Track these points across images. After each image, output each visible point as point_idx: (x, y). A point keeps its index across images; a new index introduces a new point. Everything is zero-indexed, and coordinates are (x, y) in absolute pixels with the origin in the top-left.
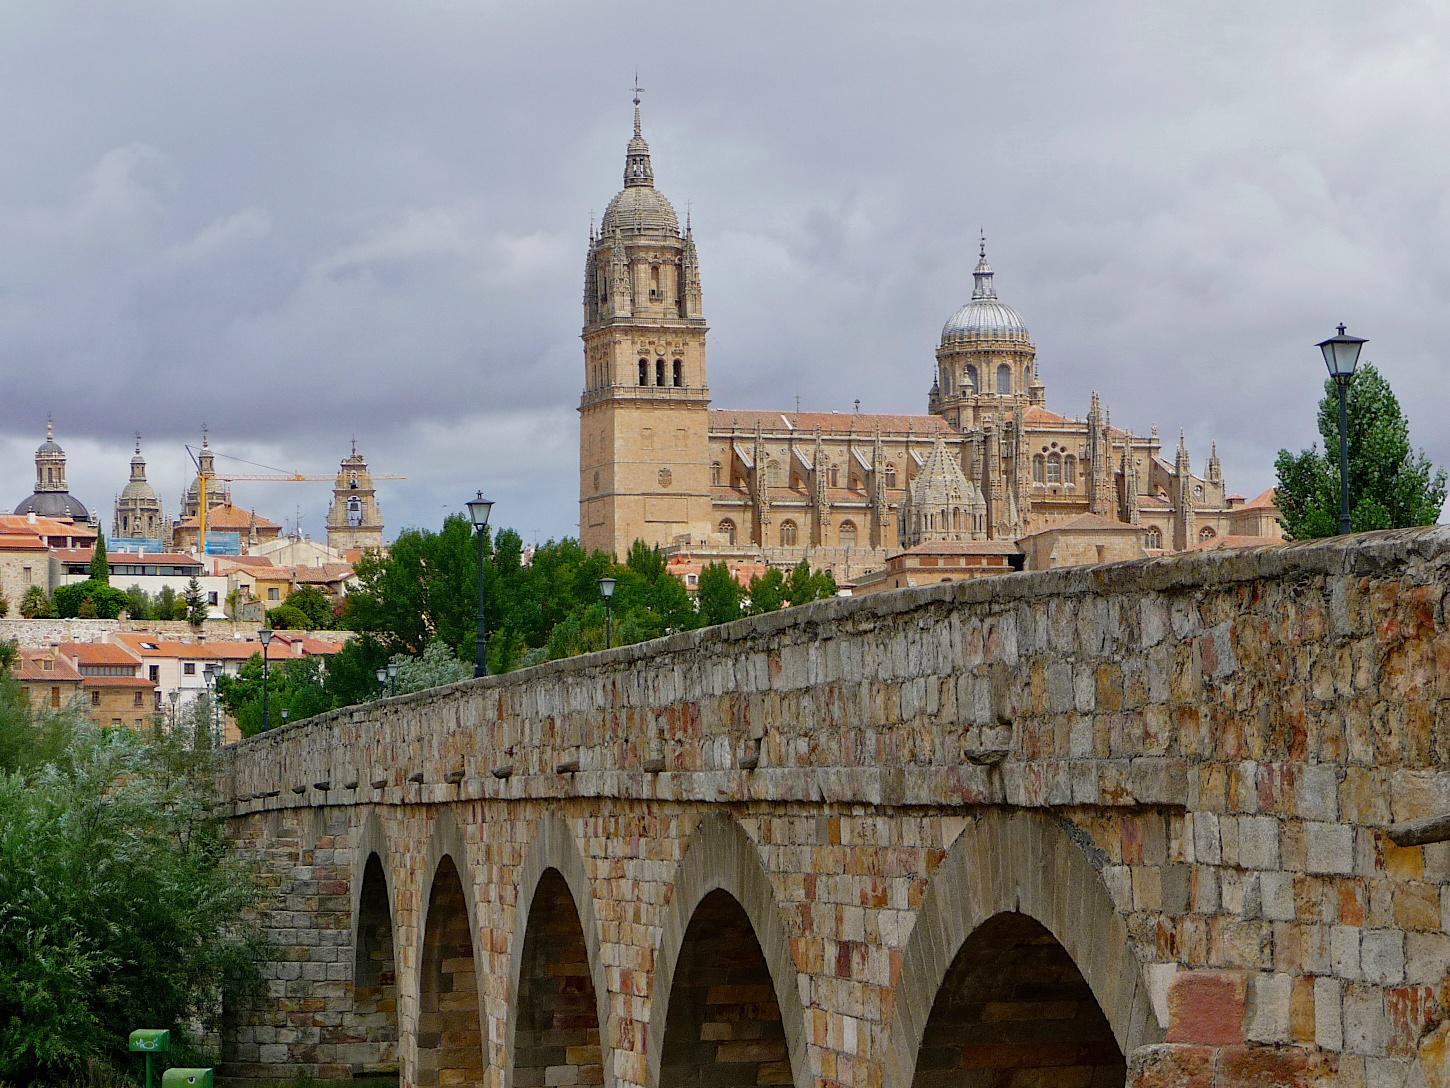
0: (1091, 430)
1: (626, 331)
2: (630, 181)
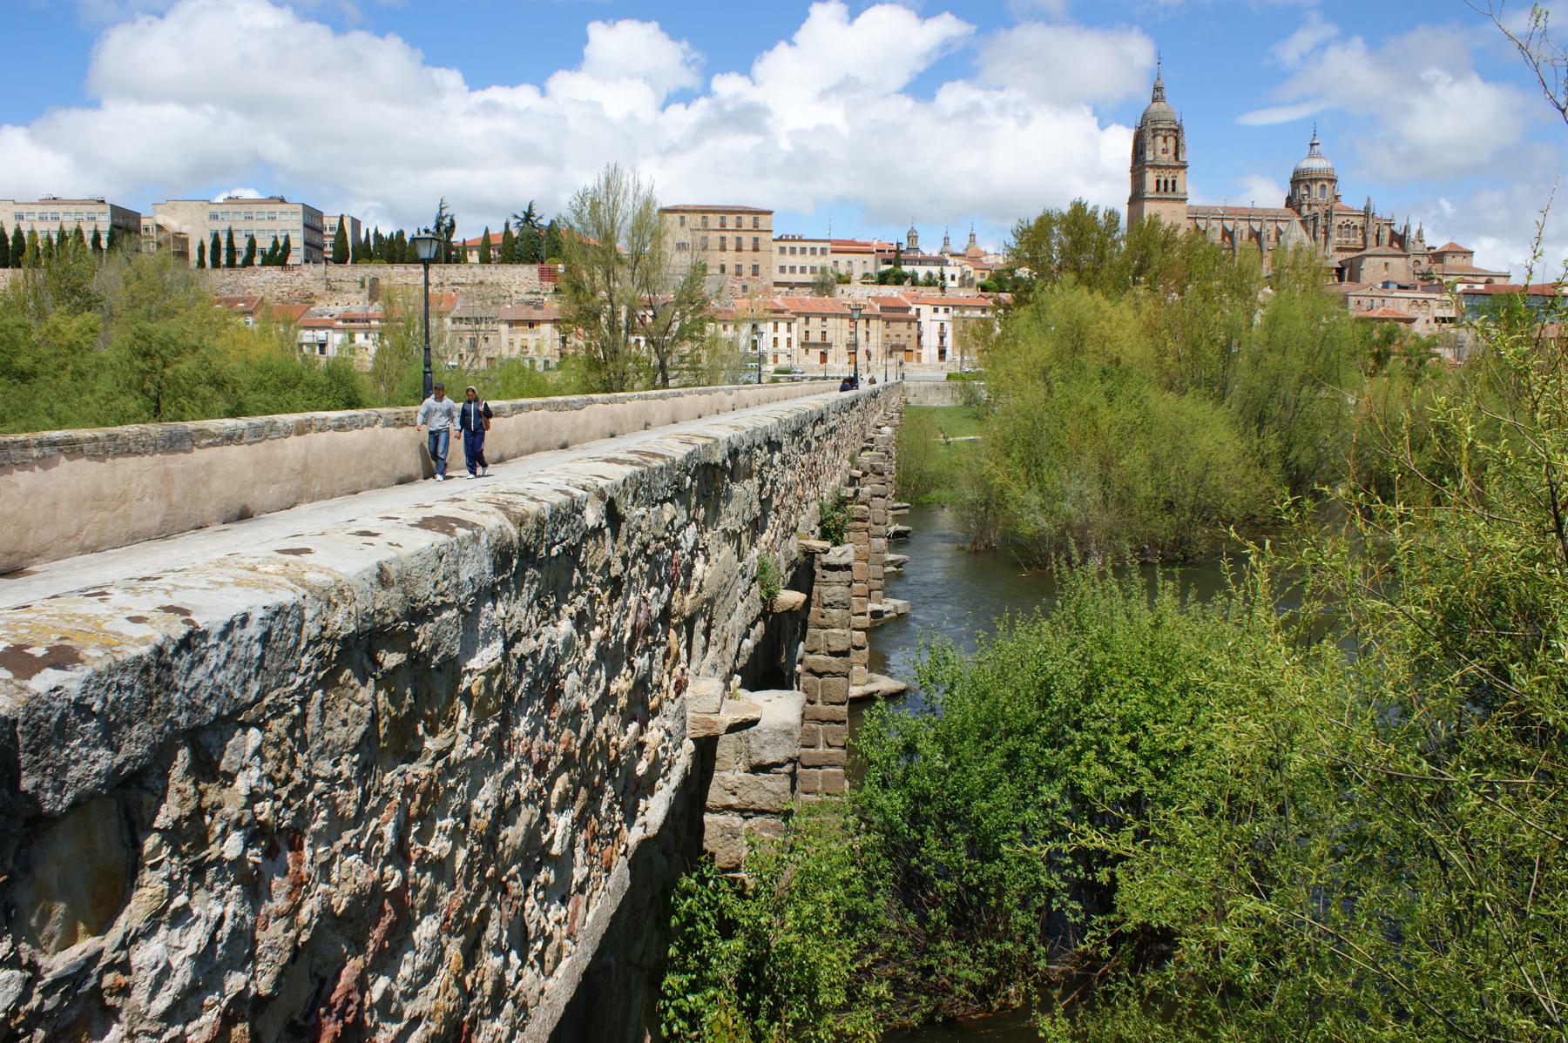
0: (1367, 214)
1: (1151, 167)
2: (1154, 100)
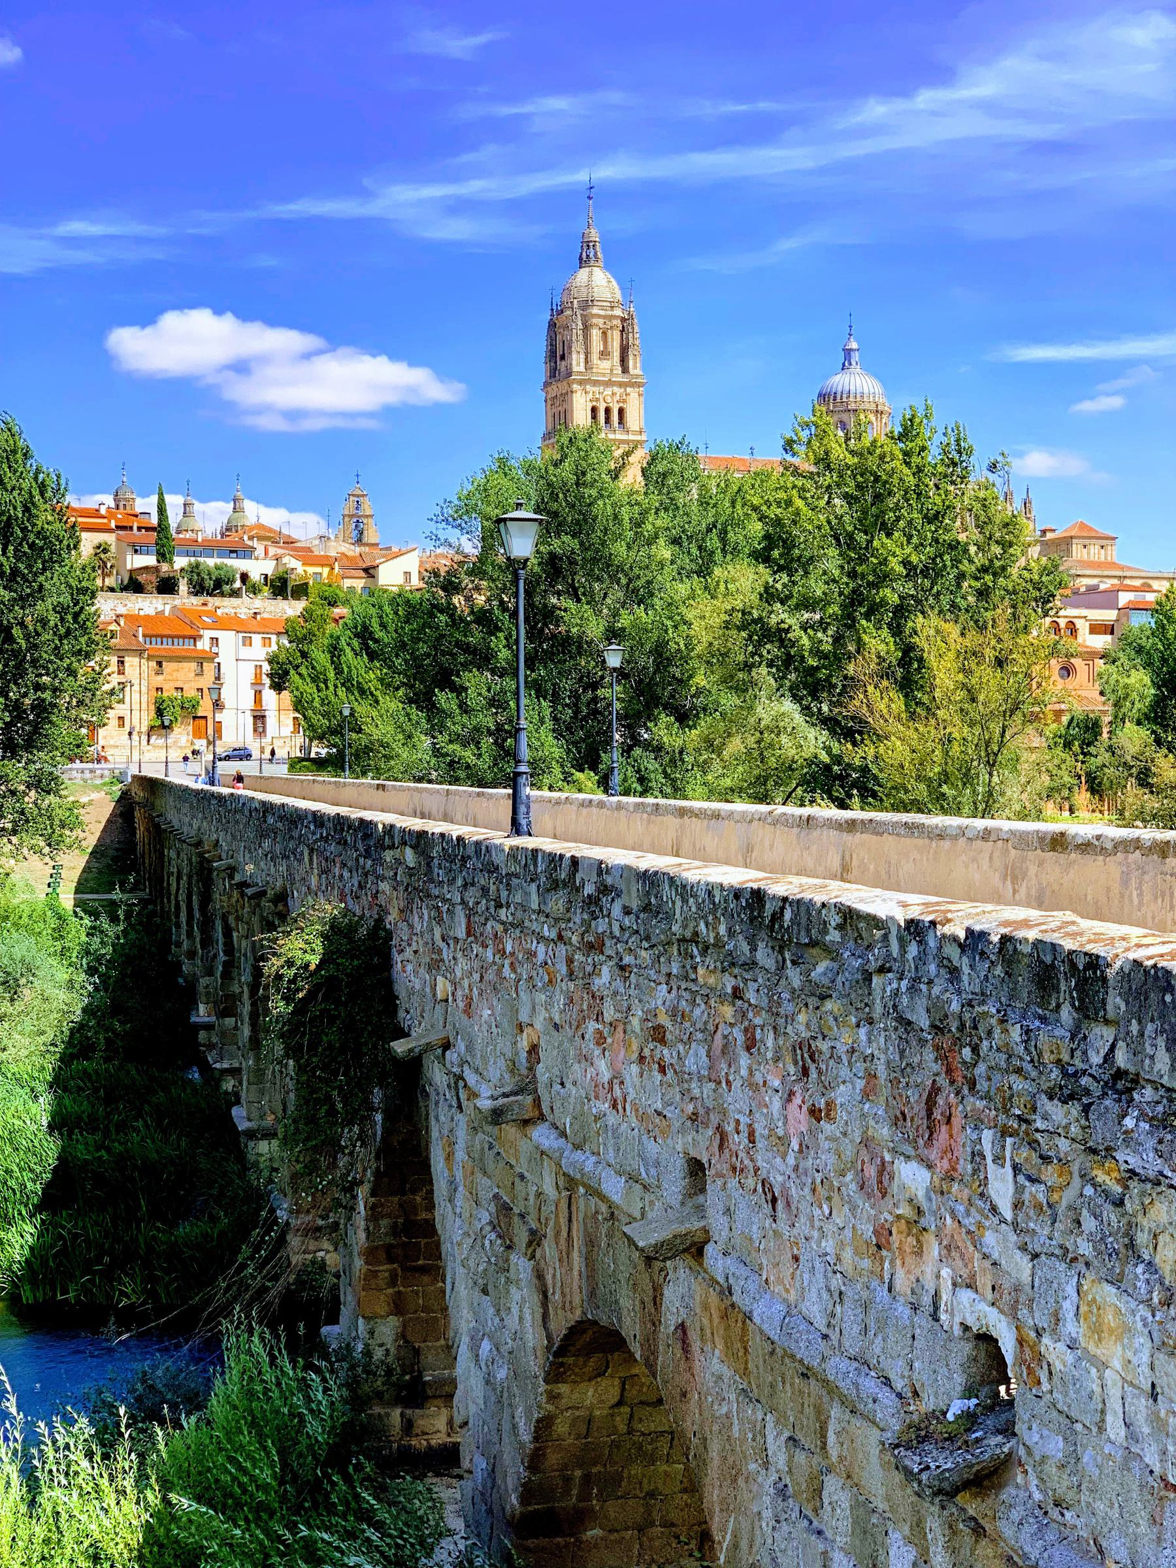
1: (581, 383)
